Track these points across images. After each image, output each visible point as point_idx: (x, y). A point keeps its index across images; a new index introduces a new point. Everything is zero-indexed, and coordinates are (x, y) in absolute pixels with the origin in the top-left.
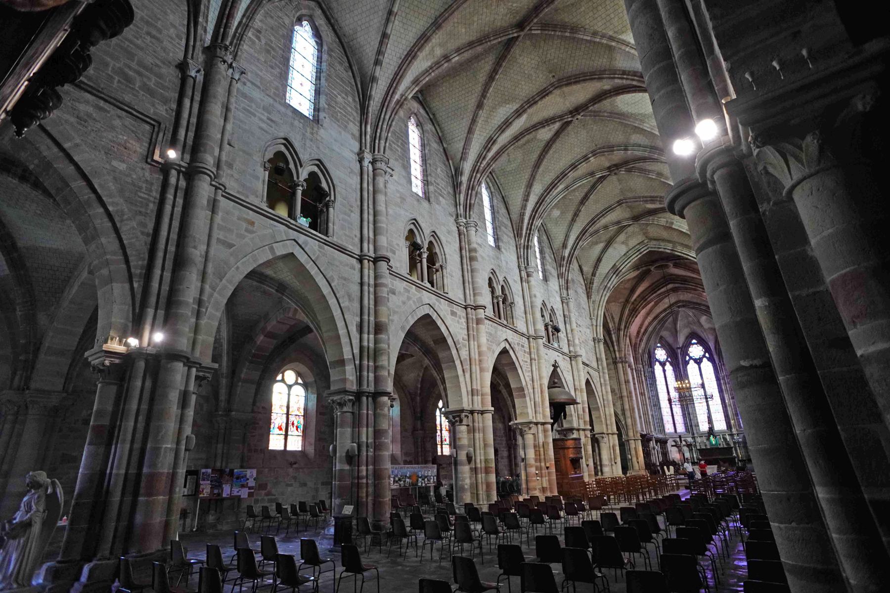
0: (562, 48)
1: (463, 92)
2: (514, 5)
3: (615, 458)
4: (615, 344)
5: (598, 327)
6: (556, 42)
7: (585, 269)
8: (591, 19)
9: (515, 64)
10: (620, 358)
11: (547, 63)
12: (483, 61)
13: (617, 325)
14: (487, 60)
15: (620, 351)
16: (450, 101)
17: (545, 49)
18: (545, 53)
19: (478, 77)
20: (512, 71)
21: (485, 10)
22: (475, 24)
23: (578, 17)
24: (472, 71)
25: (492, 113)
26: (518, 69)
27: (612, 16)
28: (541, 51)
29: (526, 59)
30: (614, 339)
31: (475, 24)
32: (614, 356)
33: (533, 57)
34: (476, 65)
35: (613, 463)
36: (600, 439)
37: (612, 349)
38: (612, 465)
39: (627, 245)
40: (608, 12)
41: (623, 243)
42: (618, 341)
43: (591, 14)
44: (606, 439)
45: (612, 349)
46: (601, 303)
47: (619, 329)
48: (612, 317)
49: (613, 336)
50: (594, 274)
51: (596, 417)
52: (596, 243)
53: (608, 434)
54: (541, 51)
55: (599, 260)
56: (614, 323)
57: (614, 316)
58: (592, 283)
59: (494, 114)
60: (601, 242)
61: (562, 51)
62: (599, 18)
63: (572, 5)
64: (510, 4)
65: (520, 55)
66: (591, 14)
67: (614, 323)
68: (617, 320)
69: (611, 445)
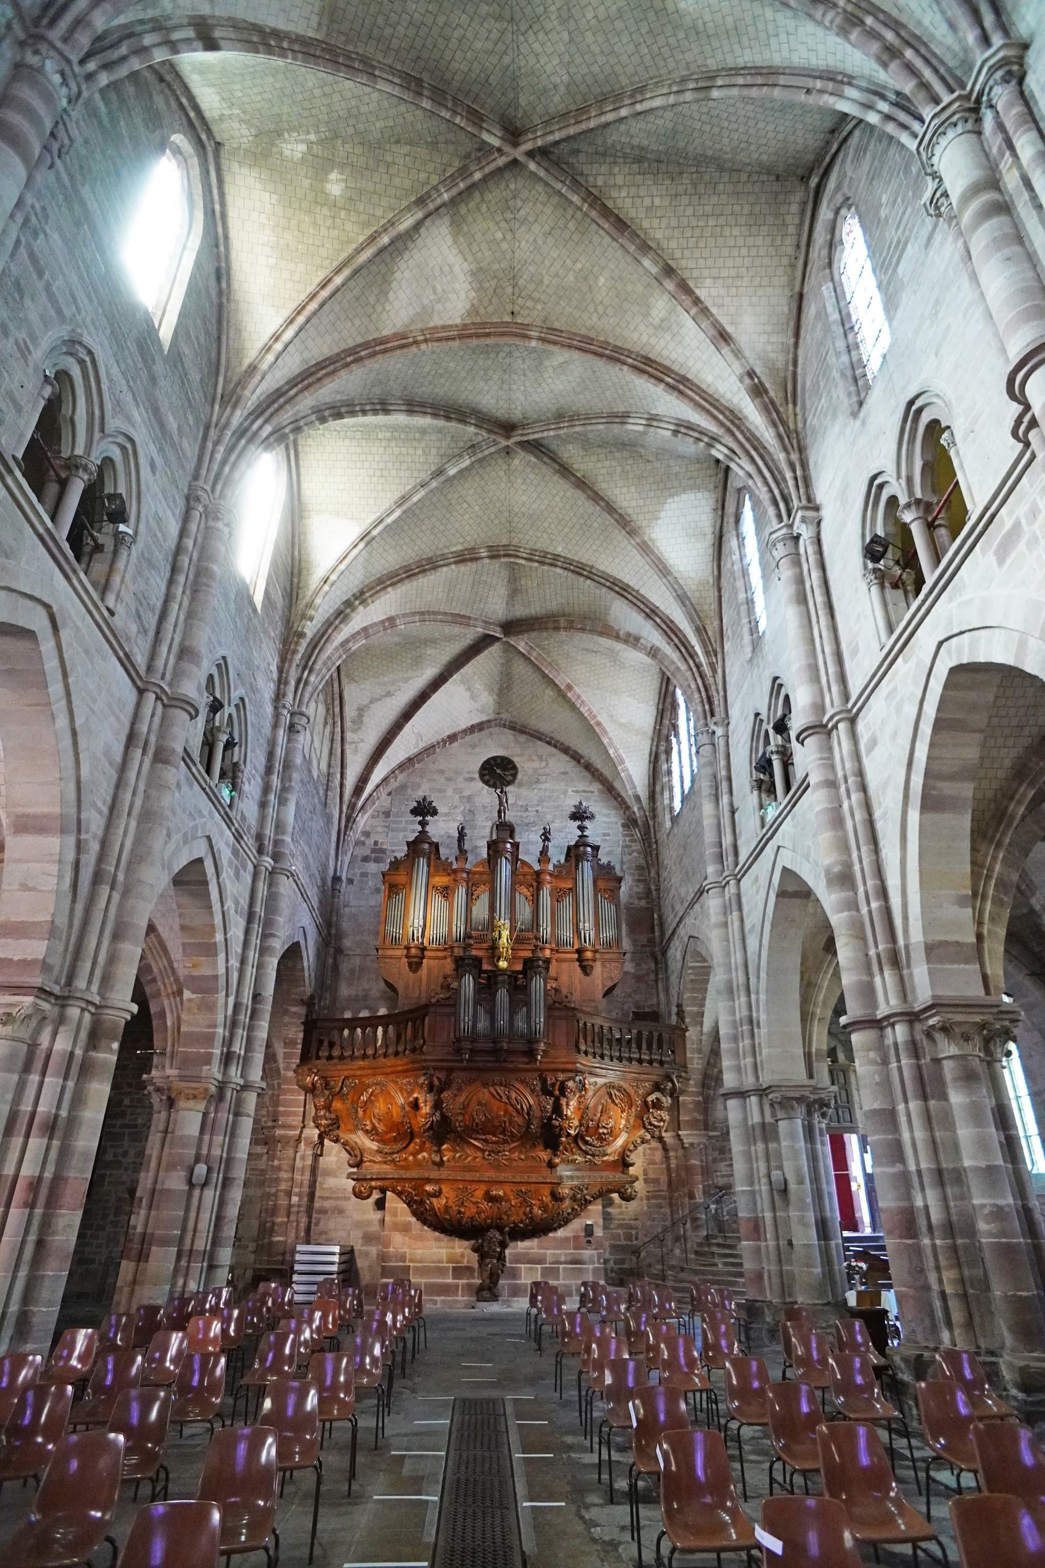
0: (454, 44)
1: (726, 124)
2: (499, 235)
6: (464, 67)
8: (366, 99)
9: (578, 78)
11: (507, 14)
12: (636, 141)
14: (625, 139)
16: (771, 127)
17: (494, 60)
18: (501, 47)
19: (670, 125)
20: (595, 69)
21: (546, 281)
22: (579, 266)
23: (392, 112)
24: (671, 143)
25: (711, 32)
26: (579, 60)
27: (317, 92)
28: (507, 60)
29: (549, 68)
31: (579, 266)
33: (532, 61)
34: (654, 147)
40: (325, 101)
43: (364, 109)
54: (507, 60)
59: (707, 17)
61: (457, 34)
62: (349, 95)
63: (398, 142)
64: (505, 246)
65: (555, 87)
66: (364, 109)
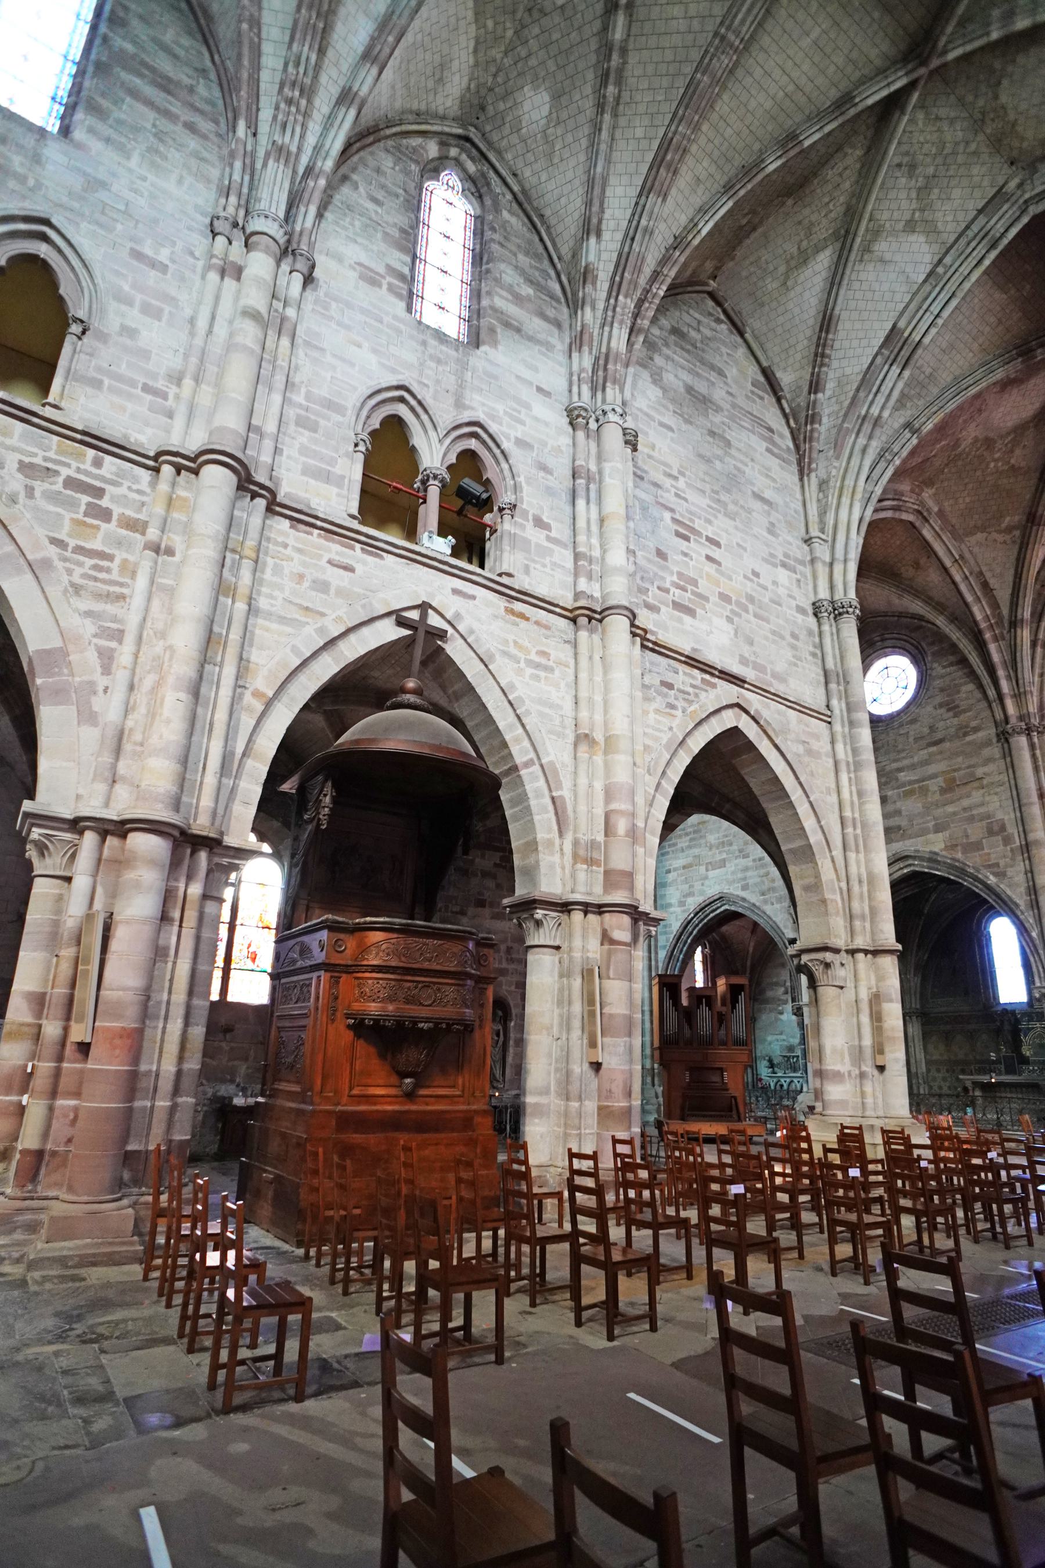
3: (879, 1049)
4: (1001, 673)
5: (838, 568)
7: (786, 378)
10: (1021, 718)
13: (1005, 611)
15: (1019, 696)
30: (996, 657)
32: (999, 715)
35: (868, 1068)
36: (818, 971)
37: (991, 693)
38: (862, 1075)
39: (931, 230)
41: (910, 226)
42: (1013, 664)
44: (840, 974)
45: (991, 693)
46: (849, 482)
47: (1014, 623)
48: (985, 585)
49: (992, 647)
50: (815, 386)
51: (807, 888)
52: (804, 258)
53: (852, 952)
55: (827, 323)
56: (995, 605)
57: (993, 582)
58: (813, 418)
60: (818, 250)
67: (995, 605)
68: (1003, 595)
69: (864, 995)
